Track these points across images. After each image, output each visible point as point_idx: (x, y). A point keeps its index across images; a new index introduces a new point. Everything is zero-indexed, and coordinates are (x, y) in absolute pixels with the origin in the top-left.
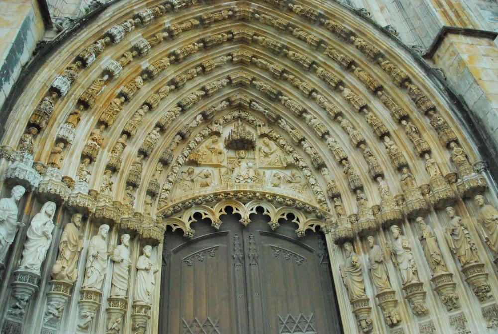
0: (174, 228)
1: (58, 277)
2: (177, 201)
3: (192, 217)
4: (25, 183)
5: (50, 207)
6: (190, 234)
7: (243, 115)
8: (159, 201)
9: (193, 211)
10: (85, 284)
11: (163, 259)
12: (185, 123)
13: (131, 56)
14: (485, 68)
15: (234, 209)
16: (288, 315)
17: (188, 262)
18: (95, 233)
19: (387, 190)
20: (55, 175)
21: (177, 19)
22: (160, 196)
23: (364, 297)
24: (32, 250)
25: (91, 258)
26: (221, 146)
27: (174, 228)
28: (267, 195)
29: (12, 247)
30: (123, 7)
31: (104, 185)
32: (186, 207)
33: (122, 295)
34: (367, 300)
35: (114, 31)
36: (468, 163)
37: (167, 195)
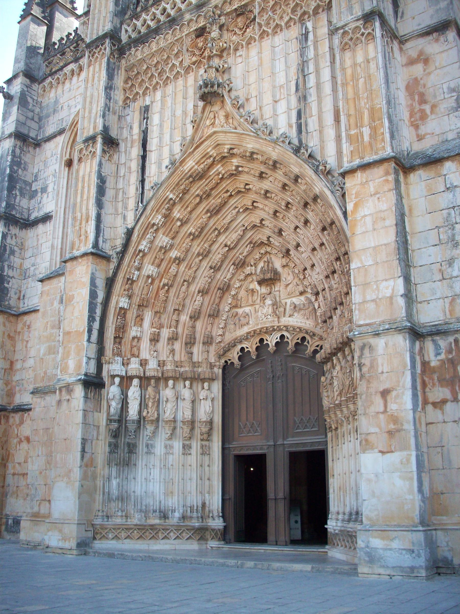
0: (229, 362)
2: (226, 343)
4: (118, 376)
5: (136, 382)
7: (269, 249)
9: (239, 347)
12: (222, 278)
13: (162, 254)
14: (366, 216)
18: (167, 386)
21: (182, 207)
26: (255, 285)
27: (229, 362)
30: (143, 223)
32: (233, 345)
35: (142, 247)
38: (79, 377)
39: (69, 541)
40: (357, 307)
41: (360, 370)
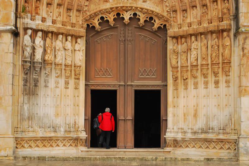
0: (91, 26)
1: (47, 61)
2: (92, 12)
3: (100, 20)
6: (99, 29)
8: (83, 12)
9: (100, 16)
10: (56, 61)
11: (86, 41)
15: (121, 15)
16: (144, 69)
17: (98, 42)
19: (196, 16)
20: (39, 19)
22: (83, 9)
23: (176, 66)
24: (37, 53)
25: (57, 51)
27: (91, 26)
28: (138, 8)
29: (31, 53)
31: (57, 15)
32: (96, 15)
33: (70, 63)
34: (178, 67)
36: (228, 14)
37: (86, 9)
38: (9, 27)
39: (5, 150)
40: (243, 15)
41: (243, 51)
